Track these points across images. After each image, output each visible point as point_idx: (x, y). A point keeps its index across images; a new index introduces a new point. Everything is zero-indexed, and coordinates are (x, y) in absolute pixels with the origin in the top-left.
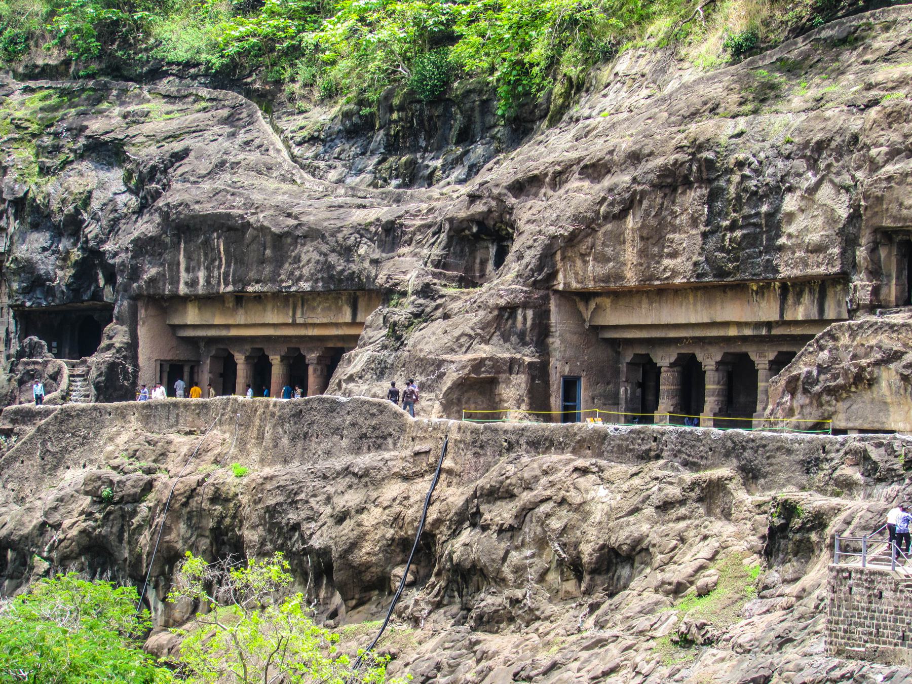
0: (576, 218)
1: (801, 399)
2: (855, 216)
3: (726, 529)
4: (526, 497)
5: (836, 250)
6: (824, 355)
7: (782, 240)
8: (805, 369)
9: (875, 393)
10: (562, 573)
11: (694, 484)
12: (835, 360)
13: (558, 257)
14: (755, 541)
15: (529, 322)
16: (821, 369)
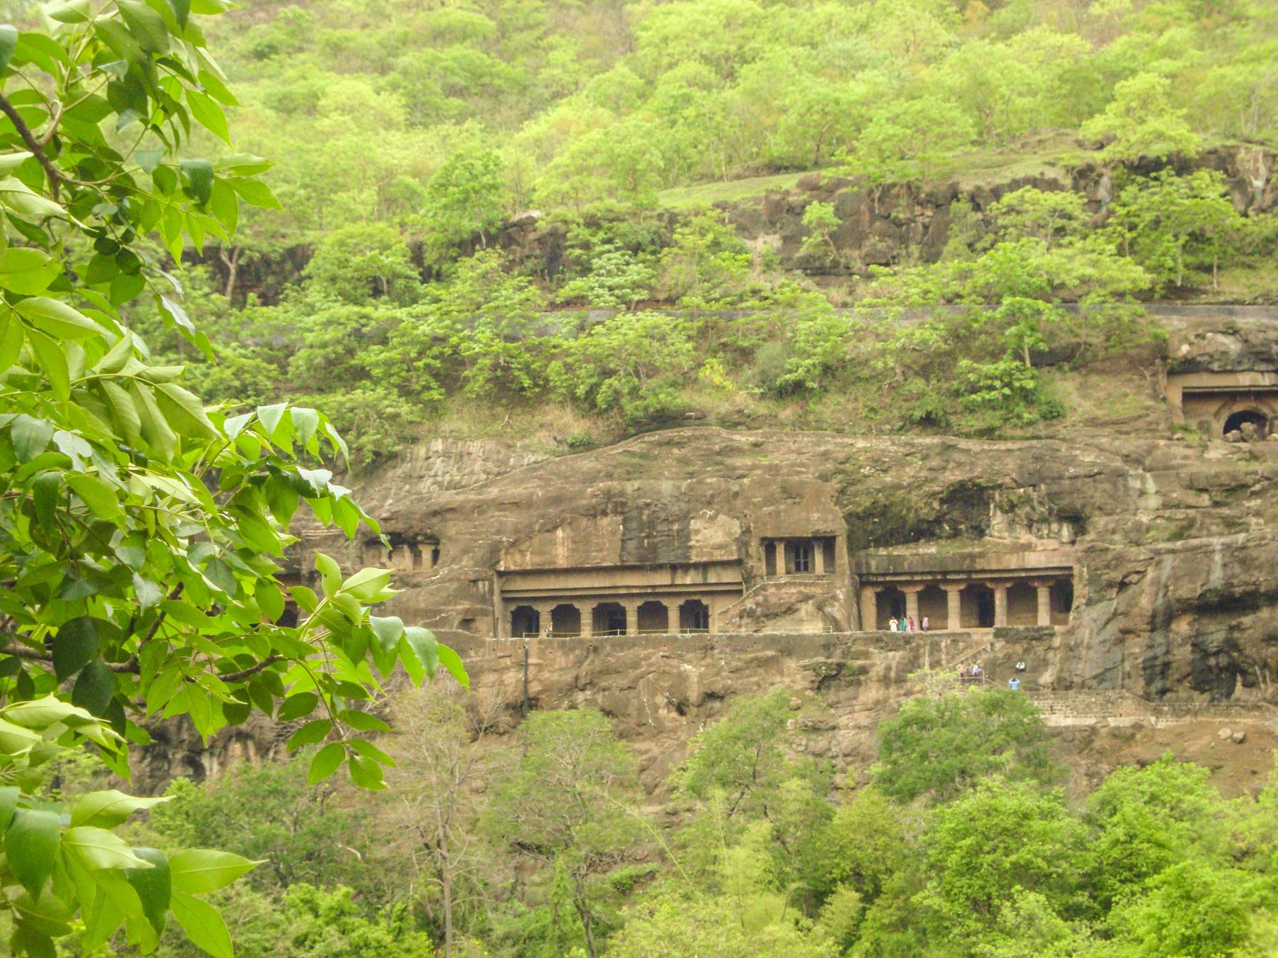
0: (517, 531)
1: (745, 620)
2: (747, 531)
3: (787, 680)
4: (633, 674)
6: (760, 598)
9: (796, 616)
11: (752, 660)
12: (766, 600)
14: (806, 684)
16: (758, 604)
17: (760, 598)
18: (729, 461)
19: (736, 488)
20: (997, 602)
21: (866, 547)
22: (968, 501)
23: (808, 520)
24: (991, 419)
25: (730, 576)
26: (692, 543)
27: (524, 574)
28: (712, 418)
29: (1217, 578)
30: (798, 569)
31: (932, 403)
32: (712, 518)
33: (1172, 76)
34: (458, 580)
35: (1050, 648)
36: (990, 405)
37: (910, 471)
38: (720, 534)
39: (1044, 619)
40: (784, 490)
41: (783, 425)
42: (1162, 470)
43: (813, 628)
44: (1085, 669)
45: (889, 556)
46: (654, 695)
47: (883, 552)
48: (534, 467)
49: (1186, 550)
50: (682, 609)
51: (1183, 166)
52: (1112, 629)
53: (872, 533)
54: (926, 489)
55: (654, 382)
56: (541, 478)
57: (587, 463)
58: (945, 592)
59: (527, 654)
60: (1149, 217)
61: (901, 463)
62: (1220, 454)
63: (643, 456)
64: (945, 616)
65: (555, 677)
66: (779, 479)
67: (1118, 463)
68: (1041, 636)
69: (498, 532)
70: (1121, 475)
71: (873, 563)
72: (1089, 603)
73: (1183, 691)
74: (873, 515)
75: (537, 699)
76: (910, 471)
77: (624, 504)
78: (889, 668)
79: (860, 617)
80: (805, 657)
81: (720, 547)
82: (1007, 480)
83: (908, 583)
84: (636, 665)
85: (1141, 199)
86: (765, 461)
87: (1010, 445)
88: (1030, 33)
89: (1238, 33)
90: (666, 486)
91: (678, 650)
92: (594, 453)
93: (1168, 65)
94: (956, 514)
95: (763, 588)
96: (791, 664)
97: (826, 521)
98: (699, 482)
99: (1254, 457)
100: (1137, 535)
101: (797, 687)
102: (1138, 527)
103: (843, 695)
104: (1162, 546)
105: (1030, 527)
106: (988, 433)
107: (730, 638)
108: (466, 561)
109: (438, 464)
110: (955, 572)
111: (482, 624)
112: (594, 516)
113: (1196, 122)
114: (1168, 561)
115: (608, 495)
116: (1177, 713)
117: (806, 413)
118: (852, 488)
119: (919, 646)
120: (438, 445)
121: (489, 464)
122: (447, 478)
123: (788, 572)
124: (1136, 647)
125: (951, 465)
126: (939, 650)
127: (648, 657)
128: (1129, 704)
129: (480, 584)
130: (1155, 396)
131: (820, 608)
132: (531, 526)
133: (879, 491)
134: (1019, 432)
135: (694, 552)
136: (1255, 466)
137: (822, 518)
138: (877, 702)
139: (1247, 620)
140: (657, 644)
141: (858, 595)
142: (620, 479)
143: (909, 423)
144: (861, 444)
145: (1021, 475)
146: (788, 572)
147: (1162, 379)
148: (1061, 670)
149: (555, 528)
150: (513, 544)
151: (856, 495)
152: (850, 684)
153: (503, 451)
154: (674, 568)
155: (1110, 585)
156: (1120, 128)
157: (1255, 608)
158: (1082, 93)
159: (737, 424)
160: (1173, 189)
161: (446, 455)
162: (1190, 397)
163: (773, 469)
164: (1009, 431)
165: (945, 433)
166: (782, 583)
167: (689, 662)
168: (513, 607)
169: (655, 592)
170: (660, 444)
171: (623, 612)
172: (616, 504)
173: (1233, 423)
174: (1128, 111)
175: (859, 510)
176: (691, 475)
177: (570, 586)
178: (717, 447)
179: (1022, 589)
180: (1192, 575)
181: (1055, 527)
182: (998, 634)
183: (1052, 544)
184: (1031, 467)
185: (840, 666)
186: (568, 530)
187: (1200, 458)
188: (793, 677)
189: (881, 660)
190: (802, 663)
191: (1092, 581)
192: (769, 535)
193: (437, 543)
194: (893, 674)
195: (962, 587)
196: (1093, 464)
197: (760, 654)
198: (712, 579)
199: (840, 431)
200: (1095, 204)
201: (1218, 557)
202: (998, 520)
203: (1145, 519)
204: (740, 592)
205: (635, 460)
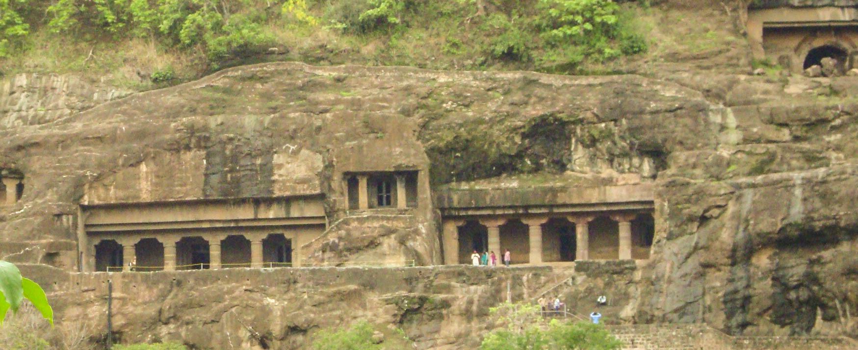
0: (100, 165)
1: (328, 254)
2: (329, 166)
3: (369, 314)
4: (216, 307)
5: (317, 182)
6: (343, 233)
7: (273, 178)
8: (332, 240)
9: (379, 250)
10: (252, 342)
11: (334, 294)
12: (349, 234)
13: (86, 187)
14: (389, 317)
15: (71, 222)
16: (340, 238)
17: (343, 233)
18: (311, 96)
19: (319, 123)
20: (579, 236)
21: (448, 181)
22: (550, 135)
23: (390, 154)
24: (573, 54)
25: (313, 211)
26: (275, 177)
27: (108, 208)
28: (295, 53)
29: (797, 212)
30: (380, 203)
31: (514, 38)
32: (295, 153)
34: (42, 214)
35: (631, 282)
36: (572, 40)
37: (492, 106)
38: (303, 168)
39: (625, 252)
40: (367, 124)
41: (365, 60)
43: (396, 262)
44: (666, 303)
45: (471, 191)
46: (237, 328)
47: (464, 186)
48: (118, 102)
49: (766, 184)
50: (265, 243)
52: (692, 264)
53: (454, 167)
54: (507, 123)
55: (237, 17)
56: (124, 113)
57: (170, 98)
58: (527, 227)
59: (110, 288)
61: (483, 97)
63: (226, 91)
64: (527, 251)
65: (139, 311)
66: (362, 114)
67: (699, 98)
68: (622, 270)
69: (83, 167)
70: (702, 109)
71: (455, 198)
72: (670, 237)
73: (764, 324)
74: (456, 150)
75: (120, 333)
76: (492, 106)
77: (207, 139)
78: (470, 302)
79: (442, 251)
80: (387, 291)
81: (303, 181)
82: (589, 115)
83: (489, 217)
84: (219, 299)
86: (347, 96)
87: (591, 80)
90: (249, 121)
91: (261, 284)
92: (178, 88)
94: (537, 149)
95: (346, 222)
96: (374, 297)
97: (408, 156)
98: (283, 117)
100: (718, 169)
101: (380, 321)
103: (425, 328)
104: (743, 180)
105: (611, 161)
106: (569, 68)
107: (313, 272)
108: (50, 196)
109: (23, 99)
110: (536, 206)
111: (66, 258)
112: (178, 151)
114: (749, 196)
115: (192, 130)
117: (389, 48)
118: (434, 123)
119: (501, 280)
120: (22, 80)
121: (73, 99)
122: (32, 112)
123: (371, 206)
124: (717, 280)
125: (533, 100)
126: (521, 284)
127: (231, 291)
129: (64, 218)
131: (402, 242)
132: (114, 160)
133: (461, 126)
134: (600, 67)
135: (277, 186)
137: (405, 152)
138: (459, 336)
139: (827, 254)
140: (240, 278)
141: (440, 230)
142: (204, 113)
143: (491, 58)
144: (443, 79)
145: (603, 110)
146: (371, 206)
148: (643, 304)
149: (139, 163)
150: (97, 179)
151: (438, 130)
152: (432, 318)
153: (87, 86)
154: (257, 202)
155: (691, 219)
157: (834, 241)
159: (319, 59)
161: (31, 90)
163: (356, 104)
164: (589, 66)
165: (526, 68)
166: (365, 218)
167: (272, 296)
168: (97, 241)
169: (239, 226)
170: (243, 79)
171: (206, 246)
172: (199, 138)
175: (442, 144)
176: (274, 110)
177: (154, 220)
178: (300, 82)
179: (603, 224)
180: (772, 209)
181: (636, 161)
182: (580, 268)
183: (633, 178)
184: (613, 102)
185: (423, 300)
186: (152, 165)
187: (781, 93)
188: (376, 310)
189: (464, 294)
190: (384, 296)
191: (673, 214)
192: (352, 169)
193: (22, 178)
194: (474, 308)
195: (544, 221)
196: (674, 99)
197: (342, 288)
198: (295, 213)
199: (422, 66)
201: (798, 192)
202: (579, 155)
203: (725, 153)
204: (322, 227)
205: (218, 95)
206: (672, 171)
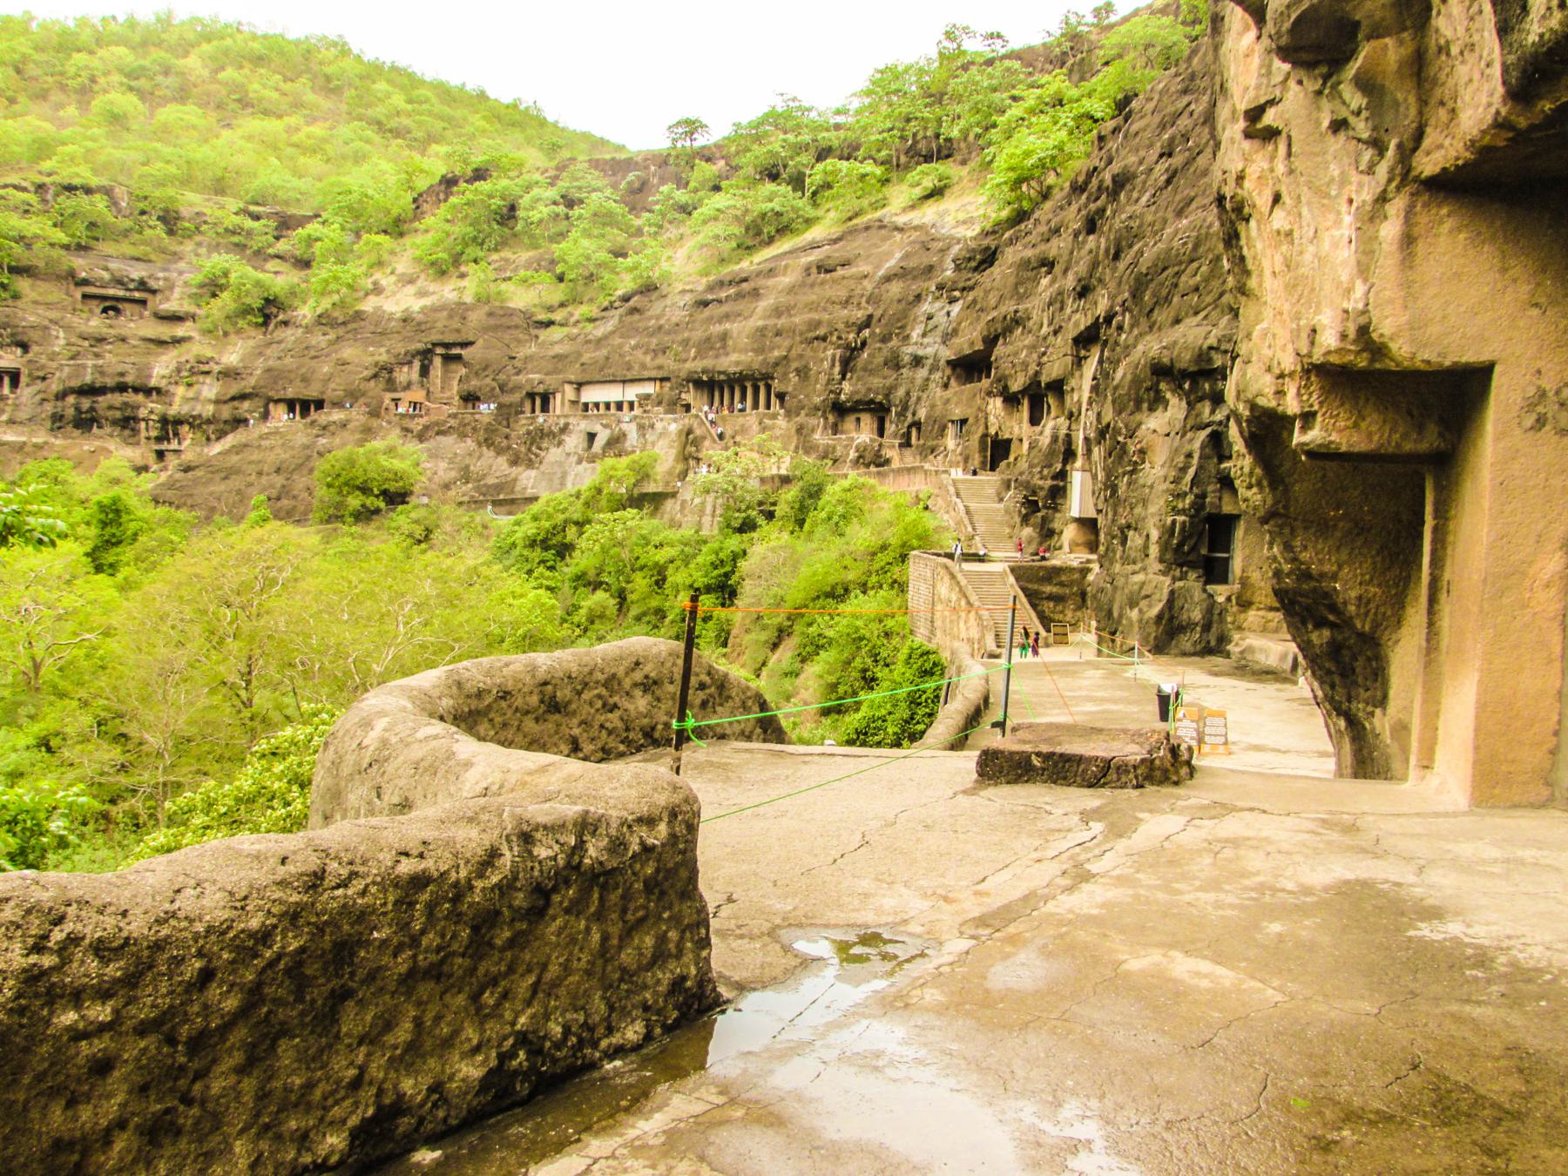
29: (88, 379)
33: (88, 151)
42: (68, 328)
44: (23, 415)
51: (88, 191)
52: (38, 397)
60: (71, 211)
62: (96, 323)
67: (46, 323)
70: (47, 328)
73: (69, 428)
85: (68, 203)
88: (29, 118)
89: (125, 134)
93: (90, 144)
99: (111, 326)
100: (53, 357)
102: (54, 353)
113: (95, 172)
114: (67, 369)
116: (65, 438)
128: (43, 432)
130: (67, 294)
136: (112, 331)
139: (100, 399)
147: (72, 287)
156: (60, 168)
158: (43, 149)
160: (82, 200)
162: (85, 296)
173: (105, 310)
174: (63, 161)
180: (77, 376)
191: (30, 375)
200: (44, 201)
203: (57, 349)
206: (30, 355)
